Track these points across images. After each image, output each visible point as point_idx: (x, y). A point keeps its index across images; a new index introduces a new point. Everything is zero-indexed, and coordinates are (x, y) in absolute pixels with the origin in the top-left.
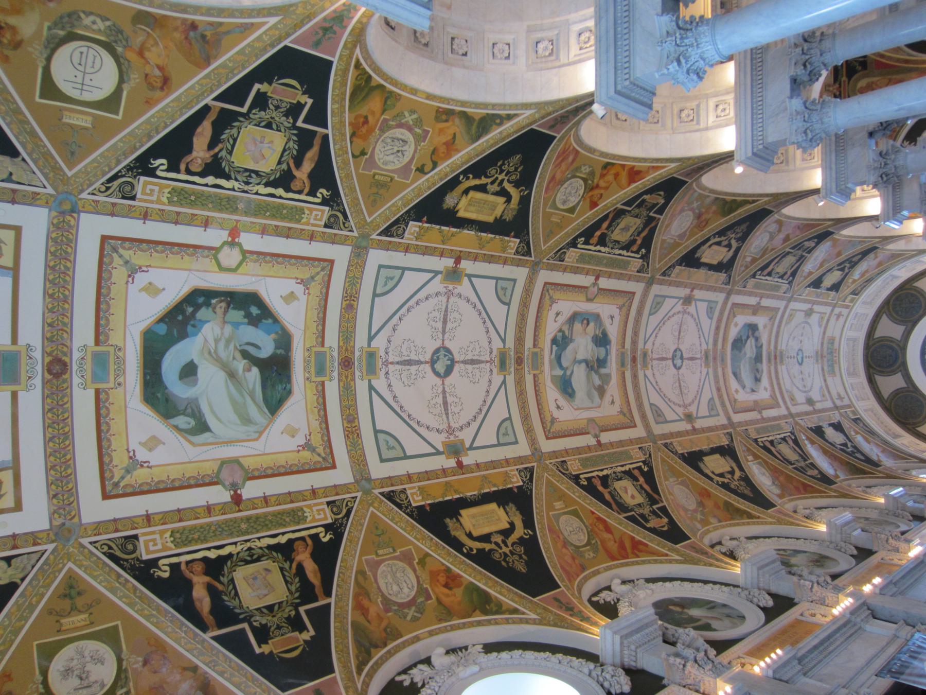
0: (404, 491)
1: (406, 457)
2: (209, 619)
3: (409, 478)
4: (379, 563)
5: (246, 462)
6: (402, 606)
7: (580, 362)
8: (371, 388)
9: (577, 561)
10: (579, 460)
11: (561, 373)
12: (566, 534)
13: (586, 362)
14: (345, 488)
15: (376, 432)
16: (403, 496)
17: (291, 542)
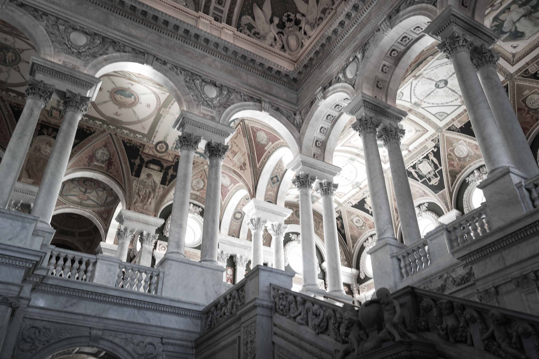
0: (453, 125)
1: (448, 115)
2: (418, 179)
3: (453, 120)
4: (454, 149)
5: (405, 143)
6: (464, 158)
7: (518, 20)
8: (423, 108)
9: (534, 118)
10: (537, 63)
11: (508, 34)
12: (529, 105)
13: (524, 16)
14: (434, 134)
15: (434, 115)
16: (453, 127)
17: (427, 155)
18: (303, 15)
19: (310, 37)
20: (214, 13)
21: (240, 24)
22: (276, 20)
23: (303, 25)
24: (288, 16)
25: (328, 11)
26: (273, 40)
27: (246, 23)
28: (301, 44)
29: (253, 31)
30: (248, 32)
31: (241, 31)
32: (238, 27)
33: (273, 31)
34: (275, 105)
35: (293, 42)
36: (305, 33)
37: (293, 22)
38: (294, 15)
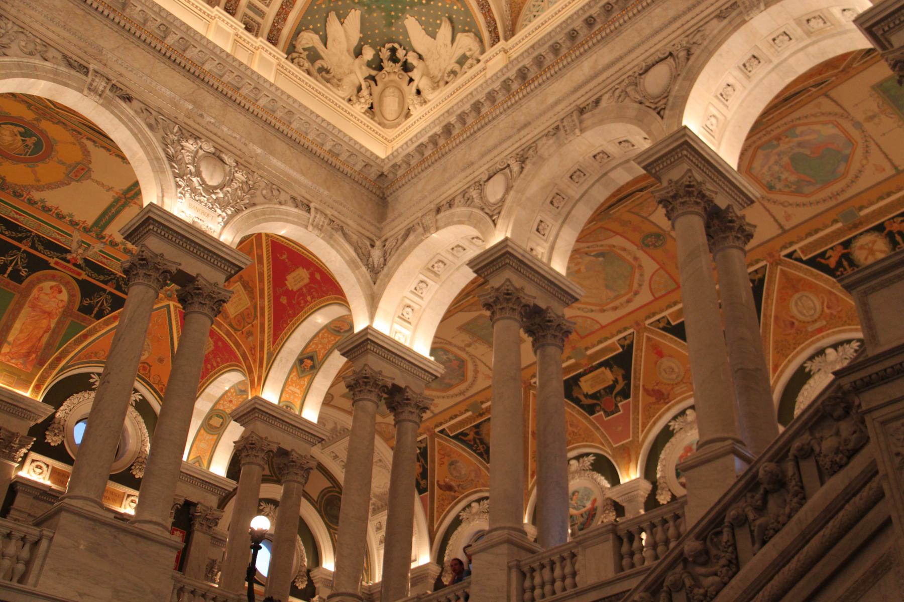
18: (420, 57)
19: (425, 102)
20: (246, 15)
21: (294, 47)
22: (369, 54)
23: (415, 74)
24: (393, 51)
25: (470, 61)
26: (355, 91)
27: (307, 46)
28: (405, 111)
29: (319, 64)
30: (307, 65)
31: (292, 61)
32: (290, 50)
33: (359, 72)
34: (336, 221)
35: (391, 105)
36: (419, 92)
37: (399, 65)
38: (404, 52)
